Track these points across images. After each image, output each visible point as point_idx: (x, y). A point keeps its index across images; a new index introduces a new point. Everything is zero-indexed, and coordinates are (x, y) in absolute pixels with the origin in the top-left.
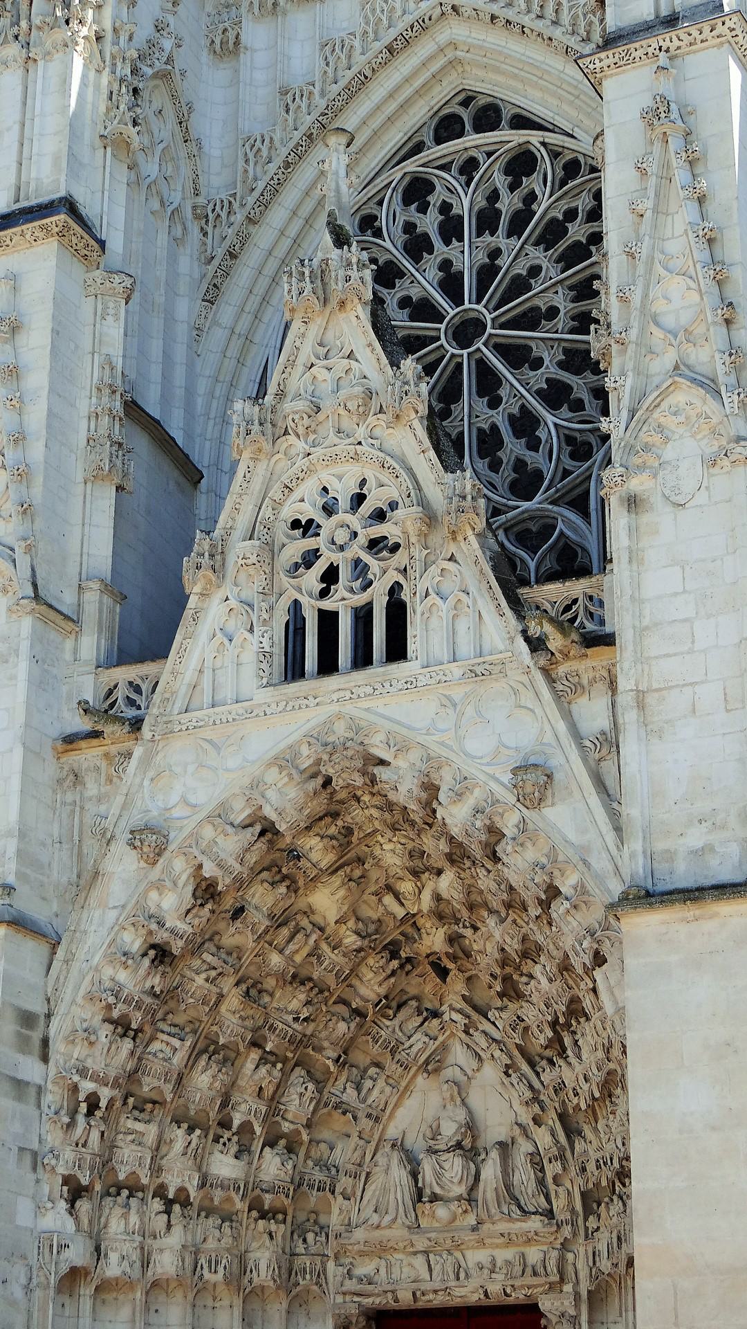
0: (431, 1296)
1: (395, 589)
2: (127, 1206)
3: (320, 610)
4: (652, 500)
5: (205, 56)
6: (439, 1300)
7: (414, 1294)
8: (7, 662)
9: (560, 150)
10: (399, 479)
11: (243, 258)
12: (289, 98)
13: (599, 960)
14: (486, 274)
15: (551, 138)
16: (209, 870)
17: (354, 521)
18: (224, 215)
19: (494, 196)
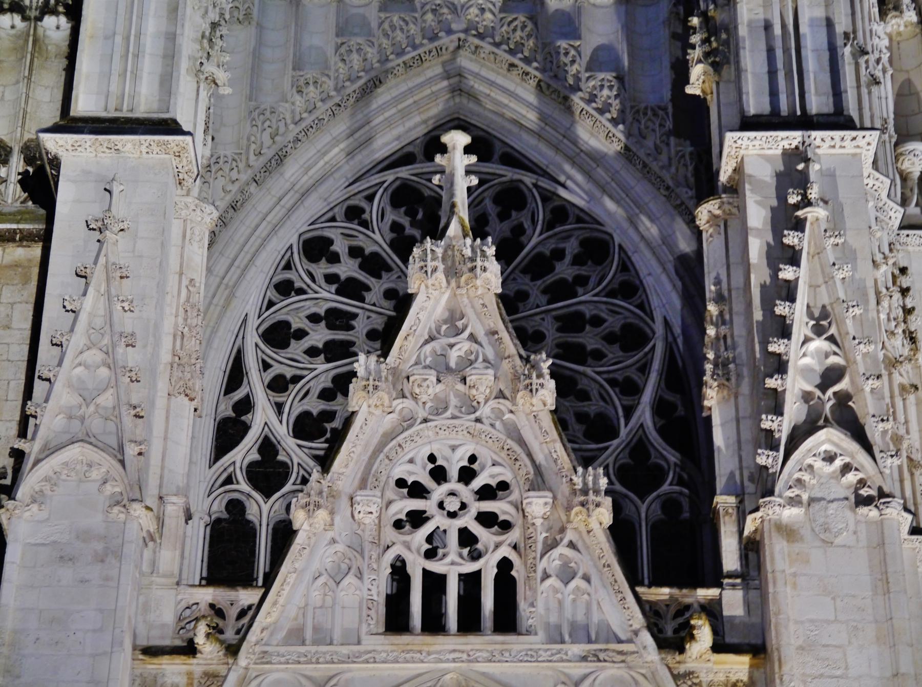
1: (505, 565)
3: (424, 570)
4: (802, 532)
9: (549, 194)
10: (518, 463)
11: (242, 214)
15: (544, 183)
17: (466, 492)
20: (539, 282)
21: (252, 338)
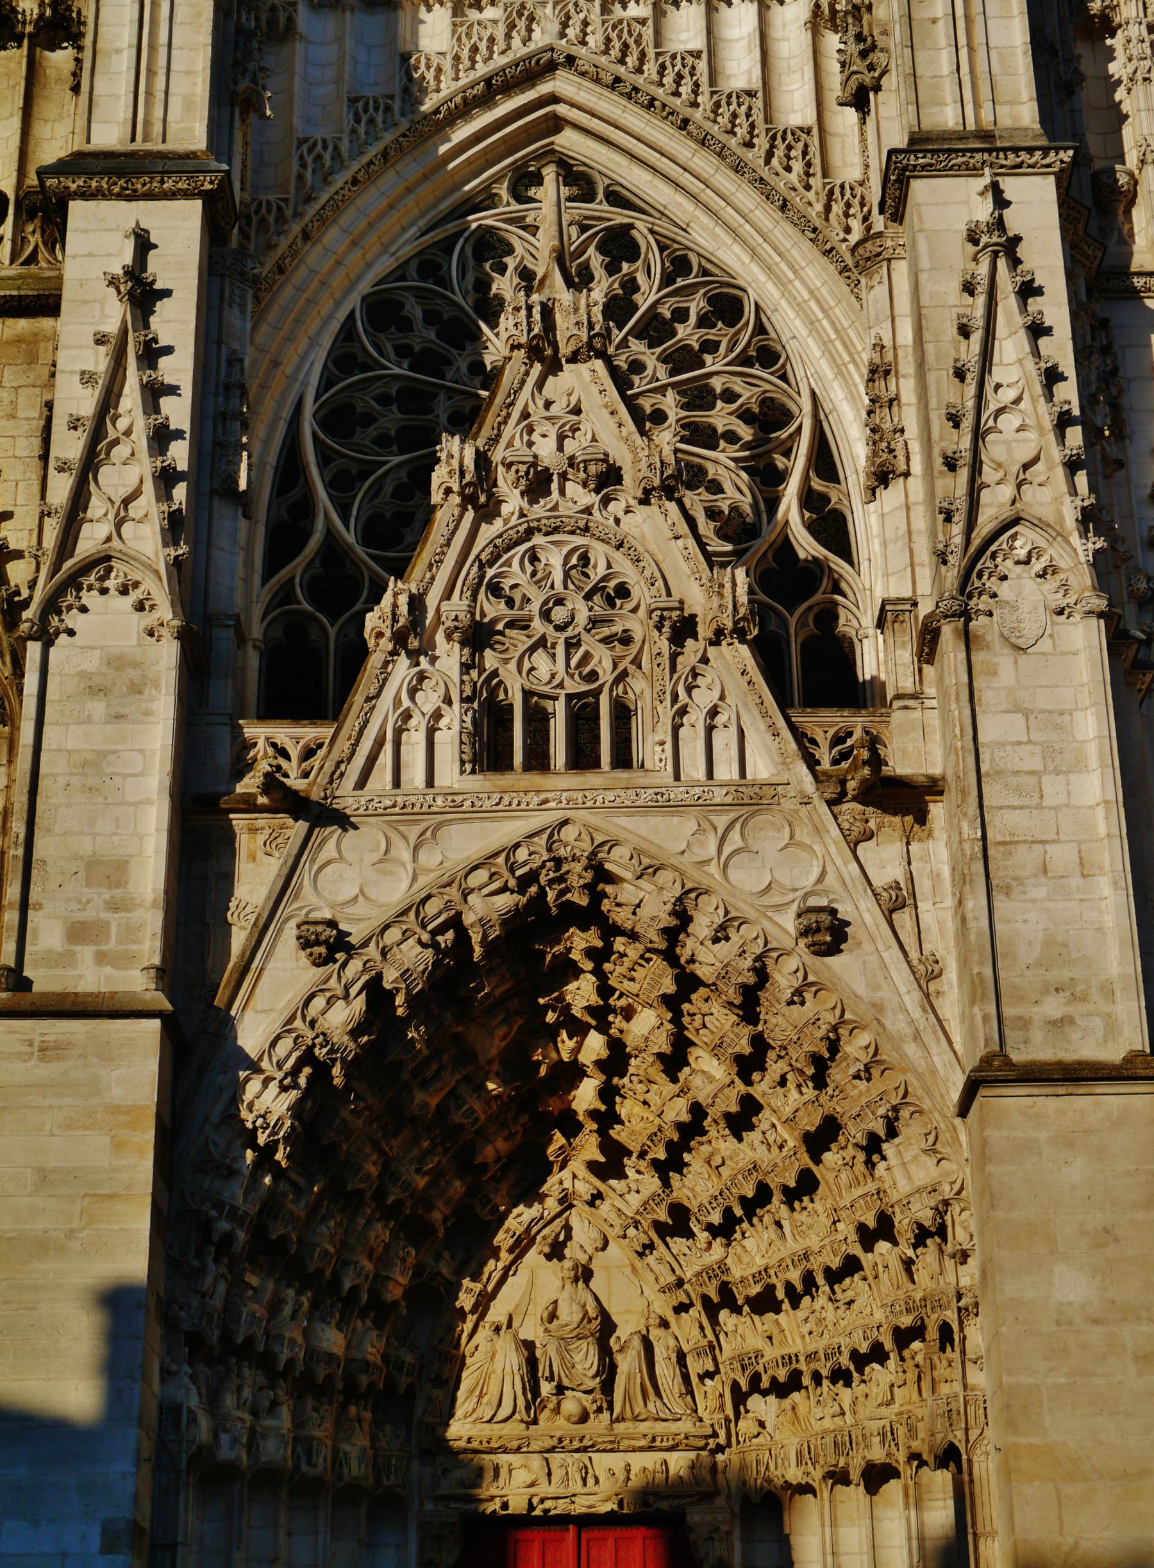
0: (548, 1504)
2: (239, 1375)
4: (988, 638)
6: (559, 1508)
7: (530, 1503)
8: (140, 692)
10: (641, 564)
12: (360, 104)
15: (664, 227)
16: (390, 978)
18: (271, 219)
20: (659, 350)
21: (308, 427)
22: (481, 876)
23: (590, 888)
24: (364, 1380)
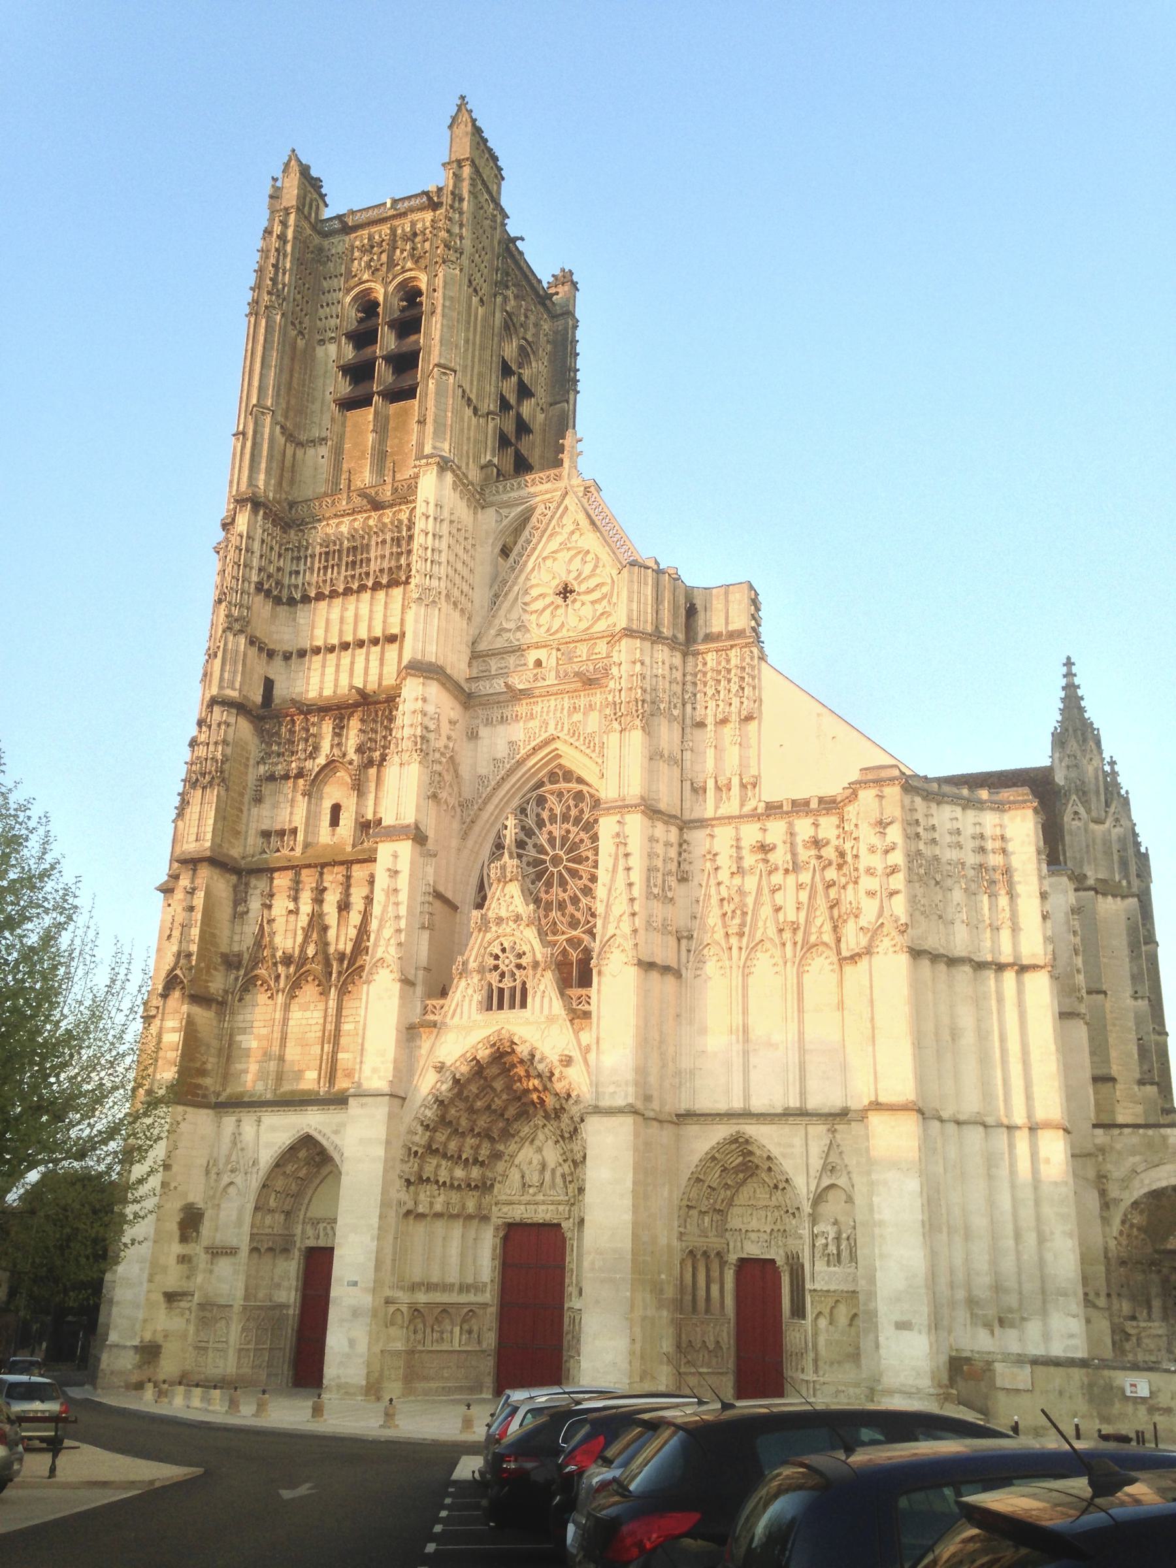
5: (465, 739)
6: (529, 1221)
13: (582, 1121)
14: (564, 839)
15: (592, 791)
16: (457, 1076)
19: (569, 808)
22: (480, 1045)
23: (510, 1046)
24: (473, 1184)
